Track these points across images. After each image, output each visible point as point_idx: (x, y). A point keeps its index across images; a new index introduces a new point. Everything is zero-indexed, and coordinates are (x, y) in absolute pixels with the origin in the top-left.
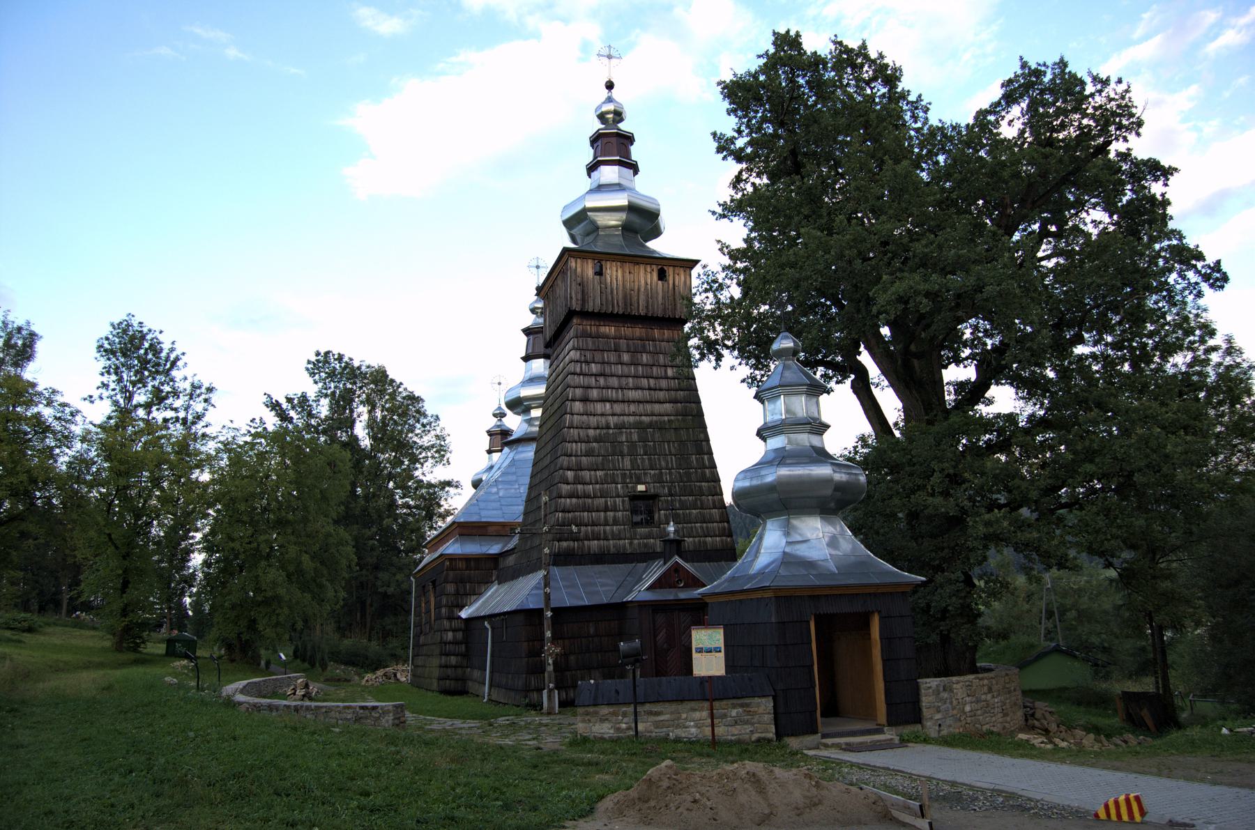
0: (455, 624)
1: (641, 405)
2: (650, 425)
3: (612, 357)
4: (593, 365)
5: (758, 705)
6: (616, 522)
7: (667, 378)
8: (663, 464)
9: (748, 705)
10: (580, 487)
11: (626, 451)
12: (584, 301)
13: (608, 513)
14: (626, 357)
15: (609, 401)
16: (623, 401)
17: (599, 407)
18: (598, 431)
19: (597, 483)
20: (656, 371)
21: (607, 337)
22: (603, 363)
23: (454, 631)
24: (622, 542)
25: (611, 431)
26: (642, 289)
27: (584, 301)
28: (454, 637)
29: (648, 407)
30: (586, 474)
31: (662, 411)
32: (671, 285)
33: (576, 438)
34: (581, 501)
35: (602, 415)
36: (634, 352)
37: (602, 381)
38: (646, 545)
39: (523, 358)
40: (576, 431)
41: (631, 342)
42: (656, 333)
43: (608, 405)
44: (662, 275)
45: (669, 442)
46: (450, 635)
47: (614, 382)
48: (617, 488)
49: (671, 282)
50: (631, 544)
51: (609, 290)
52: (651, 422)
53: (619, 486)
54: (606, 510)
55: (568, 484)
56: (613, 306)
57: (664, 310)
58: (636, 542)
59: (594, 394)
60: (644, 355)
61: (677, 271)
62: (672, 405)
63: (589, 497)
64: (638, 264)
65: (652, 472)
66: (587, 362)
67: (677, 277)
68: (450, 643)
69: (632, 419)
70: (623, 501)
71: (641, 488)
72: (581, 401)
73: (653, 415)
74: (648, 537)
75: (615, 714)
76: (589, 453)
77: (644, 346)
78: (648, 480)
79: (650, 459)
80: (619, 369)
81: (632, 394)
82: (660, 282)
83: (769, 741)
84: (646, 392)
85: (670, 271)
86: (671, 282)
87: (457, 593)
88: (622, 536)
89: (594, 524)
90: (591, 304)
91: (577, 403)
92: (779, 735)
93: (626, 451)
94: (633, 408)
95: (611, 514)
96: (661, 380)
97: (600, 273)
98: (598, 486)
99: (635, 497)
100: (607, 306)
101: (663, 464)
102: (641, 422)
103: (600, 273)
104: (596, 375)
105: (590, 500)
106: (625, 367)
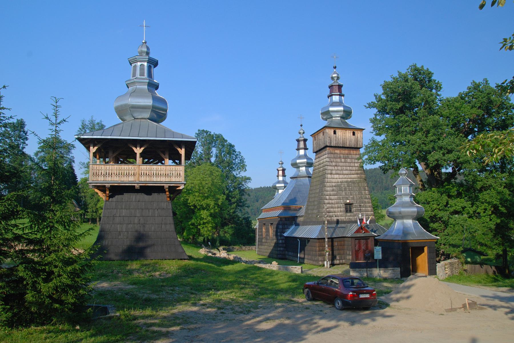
0: (282, 238)
1: (348, 175)
2: (350, 182)
3: (339, 160)
5: (396, 269)
6: (341, 212)
7: (355, 166)
8: (354, 194)
9: (394, 269)
10: (330, 201)
11: (343, 190)
12: (330, 143)
14: (343, 160)
15: (338, 174)
16: (342, 174)
17: (336, 176)
18: (335, 184)
19: (335, 200)
20: (352, 164)
21: (337, 154)
22: (336, 162)
23: (282, 240)
24: (343, 218)
25: (339, 184)
26: (348, 139)
28: (282, 242)
29: (350, 176)
30: (332, 197)
31: (354, 177)
32: (356, 137)
33: (329, 186)
34: (331, 205)
35: (336, 179)
36: (345, 158)
37: (336, 167)
38: (349, 219)
39: (296, 149)
41: (344, 155)
43: (338, 175)
44: (354, 134)
46: (281, 241)
47: (339, 168)
48: (341, 201)
49: (356, 136)
50: (345, 218)
51: (338, 139)
52: (351, 181)
53: (342, 201)
54: (338, 208)
55: (327, 200)
57: (354, 145)
58: (347, 217)
59: (334, 172)
60: (348, 159)
63: (333, 204)
64: (346, 130)
65: (351, 196)
66: (332, 162)
67: (358, 134)
68: (281, 244)
69: (345, 180)
70: (343, 205)
71: (348, 201)
73: (351, 178)
74: (350, 216)
75: (360, 271)
76: (333, 190)
77: (348, 157)
78: (350, 199)
79: (350, 192)
80: (341, 164)
81: (345, 172)
83: (399, 279)
84: (349, 171)
85: (356, 132)
87: (283, 229)
88: (343, 215)
89: (335, 212)
90: (333, 144)
91: (329, 175)
92: (401, 277)
93: (343, 190)
94: (345, 176)
95: (339, 209)
97: (335, 133)
98: (336, 201)
99: (346, 204)
100: (337, 144)
101: (354, 194)
102: (348, 181)
103: (335, 133)
105: (333, 205)
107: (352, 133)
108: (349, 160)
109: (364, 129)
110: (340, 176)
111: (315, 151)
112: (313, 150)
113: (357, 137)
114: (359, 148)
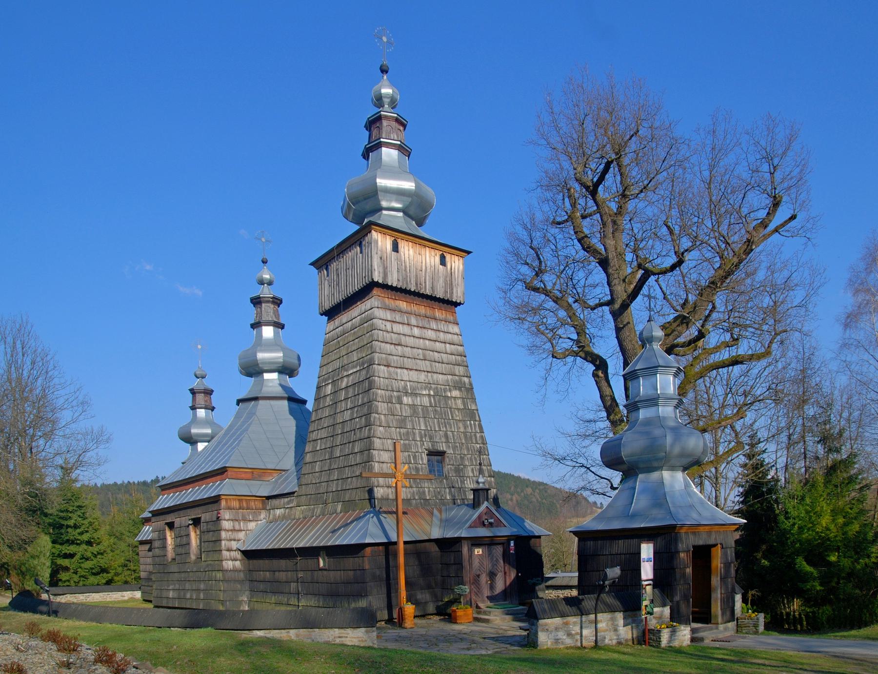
3: (406, 329)
4: (392, 334)
12: (385, 275)
13: (410, 465)
14: (416, 332)
18: (399, 393)
26: (428, 270)
27: (385, 275)
37: (399, 348)
40: (383, 392)
42: (438, 314)
44: (443, 262)
45: (450, 408)
56: (407, 283)
61: (453, 259)
62: (451, 376)
72: (385, 366)
80: (410, 341)
82: (441, 266)
85: (448, 257)
86: (449, 267)
96: (442, 354)
98: (402, 442)
104: (395, 344)
106: (415, 339)
107: (438, 259)
108: (430, 334)
109: (469, 253)
110: (411, 373)
111: (327, 306)
112: (321, 305)
113: (451, 269)
114: (456, 304)
